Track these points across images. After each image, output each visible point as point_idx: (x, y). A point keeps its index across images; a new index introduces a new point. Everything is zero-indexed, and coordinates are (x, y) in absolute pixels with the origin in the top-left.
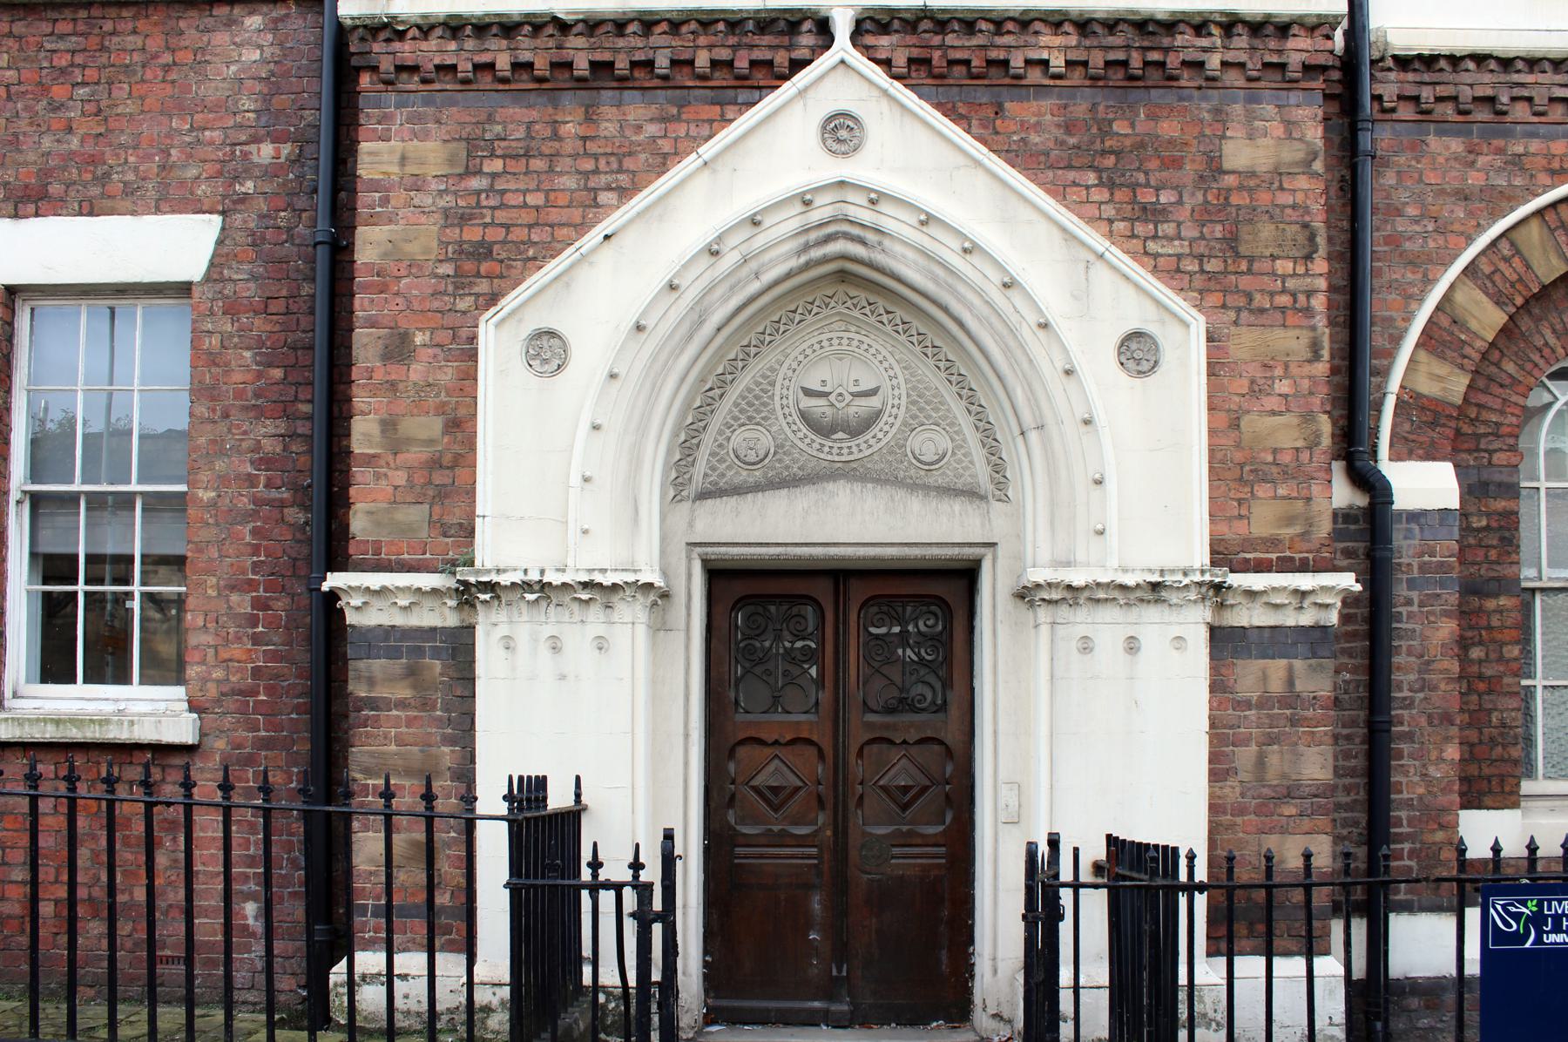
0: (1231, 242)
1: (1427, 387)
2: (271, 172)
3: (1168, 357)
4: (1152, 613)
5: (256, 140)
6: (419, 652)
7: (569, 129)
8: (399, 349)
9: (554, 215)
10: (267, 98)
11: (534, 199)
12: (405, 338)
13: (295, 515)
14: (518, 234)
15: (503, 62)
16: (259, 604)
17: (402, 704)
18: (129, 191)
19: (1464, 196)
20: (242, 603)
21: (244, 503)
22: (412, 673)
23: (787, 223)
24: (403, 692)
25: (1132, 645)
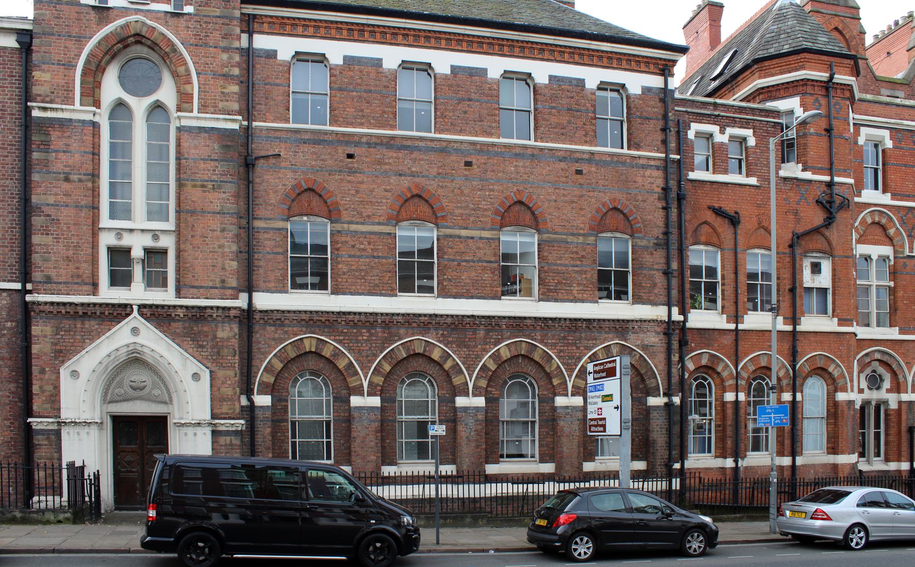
0: (218, 353)
2: (11, 329)
3: (202, 378)
4: (199, 428)
6: (49, 434)
7: (79, 326)
8: (43, 371)
9: (76, 344)
10: (9, 312)
12: (44, 369)
13: (20, 404)
14: (68, 348)
15: (63, 311)
16: (11, 423)
17: (45, 445)
20: (7, 423)
21: (7, 401)
22: (48, 439)
23: (125, 350)
24: (46, 442)
25: (195, 434)
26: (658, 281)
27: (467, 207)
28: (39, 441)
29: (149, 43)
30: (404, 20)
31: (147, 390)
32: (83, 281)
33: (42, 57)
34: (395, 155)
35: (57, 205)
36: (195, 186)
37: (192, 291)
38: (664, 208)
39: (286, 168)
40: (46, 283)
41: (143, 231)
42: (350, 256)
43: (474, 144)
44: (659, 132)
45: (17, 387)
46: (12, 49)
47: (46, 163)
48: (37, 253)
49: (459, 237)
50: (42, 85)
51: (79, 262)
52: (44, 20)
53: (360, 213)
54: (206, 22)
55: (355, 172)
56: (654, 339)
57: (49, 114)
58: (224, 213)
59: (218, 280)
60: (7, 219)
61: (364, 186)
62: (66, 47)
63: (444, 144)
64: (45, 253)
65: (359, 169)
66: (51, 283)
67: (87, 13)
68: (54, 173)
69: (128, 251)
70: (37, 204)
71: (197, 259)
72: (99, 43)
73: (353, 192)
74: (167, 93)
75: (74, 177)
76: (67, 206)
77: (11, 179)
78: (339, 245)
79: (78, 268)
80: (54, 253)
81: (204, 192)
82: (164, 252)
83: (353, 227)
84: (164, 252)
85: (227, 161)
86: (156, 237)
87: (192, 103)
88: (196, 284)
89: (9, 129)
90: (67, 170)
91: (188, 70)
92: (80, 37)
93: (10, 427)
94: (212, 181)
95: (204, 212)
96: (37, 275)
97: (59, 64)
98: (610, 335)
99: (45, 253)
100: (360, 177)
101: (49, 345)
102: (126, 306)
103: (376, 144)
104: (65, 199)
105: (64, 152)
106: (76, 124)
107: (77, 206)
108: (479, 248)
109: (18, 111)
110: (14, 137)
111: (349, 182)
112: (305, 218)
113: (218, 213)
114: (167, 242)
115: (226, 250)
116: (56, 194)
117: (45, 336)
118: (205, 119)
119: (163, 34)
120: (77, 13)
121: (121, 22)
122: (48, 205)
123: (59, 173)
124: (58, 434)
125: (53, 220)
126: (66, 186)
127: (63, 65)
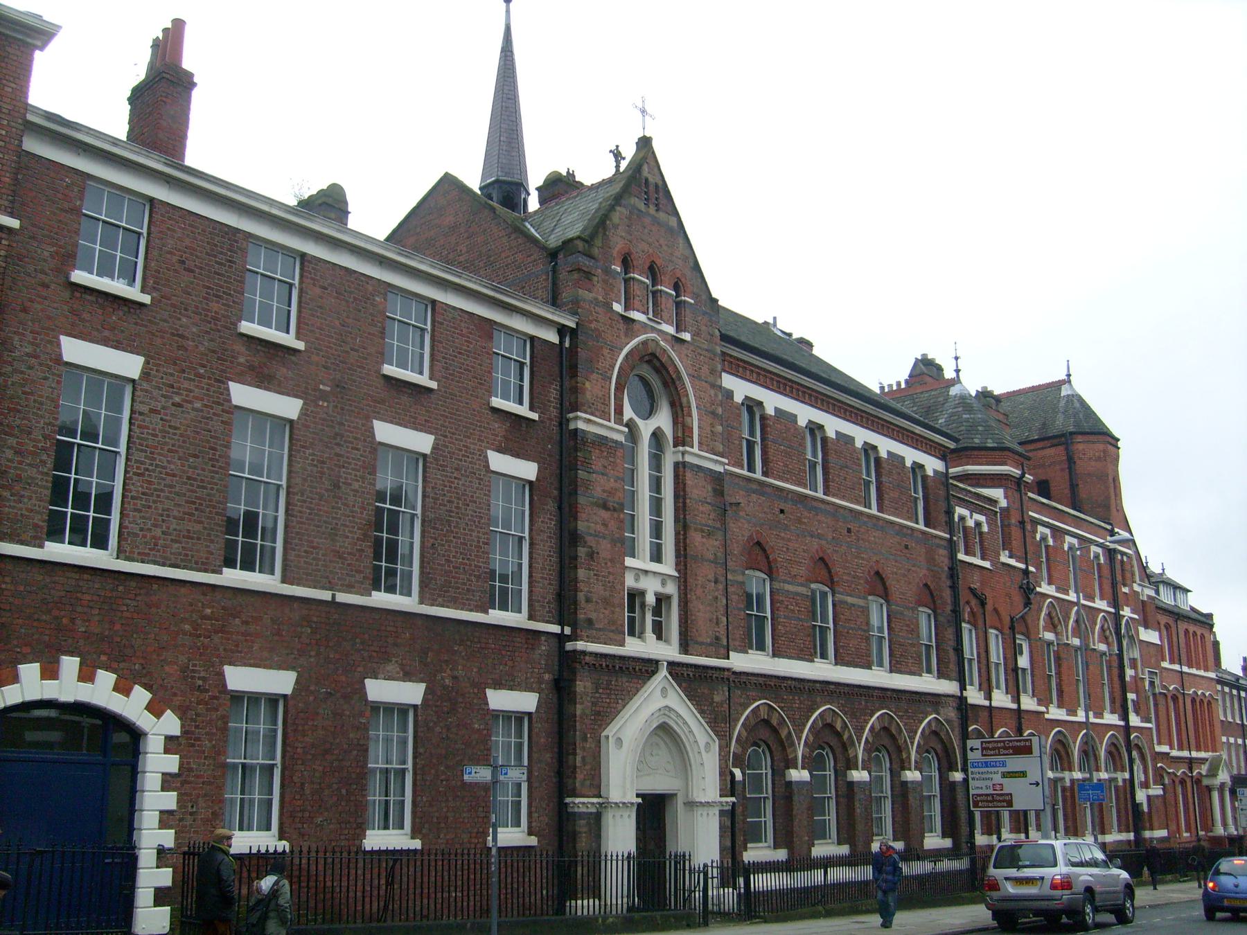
5: (544, 673)
8: (585, 739)
9: (612, 705)
11: (608, 700)
12: (586, 735)
18: (519, 684)
29: (658, 364)
32: (617, 628)
38: (950, 587)
41: (655, 573)
45: (552, 758)
49: (846, 603)
51: (613, 606)
69: (642, 593)
71: (699, 612)
72: (626, 356)
73: (785, 549)
74: (663, 420)
86: (663, 584)
91: (689, 402)
105: (603, 474)
114: (671, 589)
121: (642, 337)
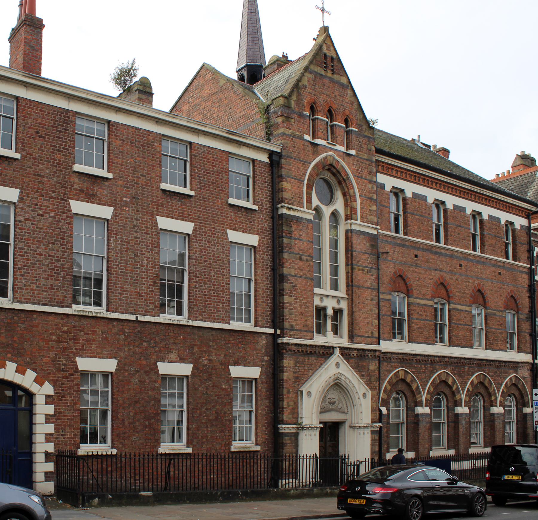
0: (370, 379)
1: (383, 397)
2: (267, 361)
3: (367, 396)
4: (366, 429)
5: (265, 356)
6: (291, 436)
7: (306, 360)
8: (289, 392)
9: (305, 373)
10: (266, 349)
11: (303, 370)
12: (289, 390)
13: (271, 415)
14: (301, 376)
15: (300, 350)
16: (266, 429)
17: (289, 443)
18: (249, 363)
19: (387, 371)
20: (264, 428)
21: (264, 413)
22: (291, 439)
23: (332, 378)
24: (289, 442)
25: (364, 434)
26: (527, 339)
27: (460, 291)
28: (286, 440)
29: (335, 171)
30: (413, 166)
31: (336, 404)
32: (308, 329)
33: (287, 172)
34: (433, 257)
35: (296, 276)
36: (359, 270)
37: (359, 338)
38: (529, 297)
39: (390, 261)
40: (291, 330)
41: (333, 297)
42: (417, 319)
43: (462, 253)
44: (526, 252)
45: (269, 403)
46: (266, 163)
47: (290, 246)
48: (286, 309)
49: (458, 309)
50: (287, 192)
51: (306, 316)
52: (287, 147)
53: (420, 292)
54: (361, 162)
55: (418, 266)
56: (526, 373)
57: (291, 213)
58: (372, 289)
59: (370, 332)
60: (265, 283)
61: (422, 276)
62: (298, 168)
63: (452, 252)
64: (290, 309)
65: (419, 264)
66: (293, 330)
67: (308, 146)
68: (294, 254)
69: (325, 309)
70: (287, 275)
71: (360, 318)
72: (314, 167)
73: (417, 279)
74: (339, 205)
75: (304, 258)
76: (301, 277)
77: (267, 255)
78: (413, 312)
79: (306, 321)
80: (295, 309)
81: (363, 274)
82: (341, 311)
83: (418, 301)
84: (341, 311)
85: (372, 255)
86: (338, 302)
87: (357, 214)
88: (360, 334)
89: (265, 219)
90: (300, 252)
91: (354, 192)
92: (305, 162)
93: (265, 431)
94: (367, 267)
95: (363, 287)
96: (287, 325)
97: (295, 179)
98: (511, 371)
99: (290, 309)
100: (420, 270)
101: (292, 374)
102: (329, 347)
103: (426, 249)
104: (300, 272)
105: (299, 240)
106: (304, 221)
107: (305, 278)
108: (465, 317)
109: (269, 207)
110: (268, 225)
111: (416, 272)
112: (396, 293)
113: (370, 288)
114: (344, 305)
115: (373, 313)
116: (296, 269)
117: (290, 367)
118: (364, 226)
119: (343, 167)
120: (303, 145)
121: (324, 155)
122: (292, 276)
123: (297, 254)
124: (296, 435)
125: (294, 286)
126: (300, 263)
127: (297, 179)
